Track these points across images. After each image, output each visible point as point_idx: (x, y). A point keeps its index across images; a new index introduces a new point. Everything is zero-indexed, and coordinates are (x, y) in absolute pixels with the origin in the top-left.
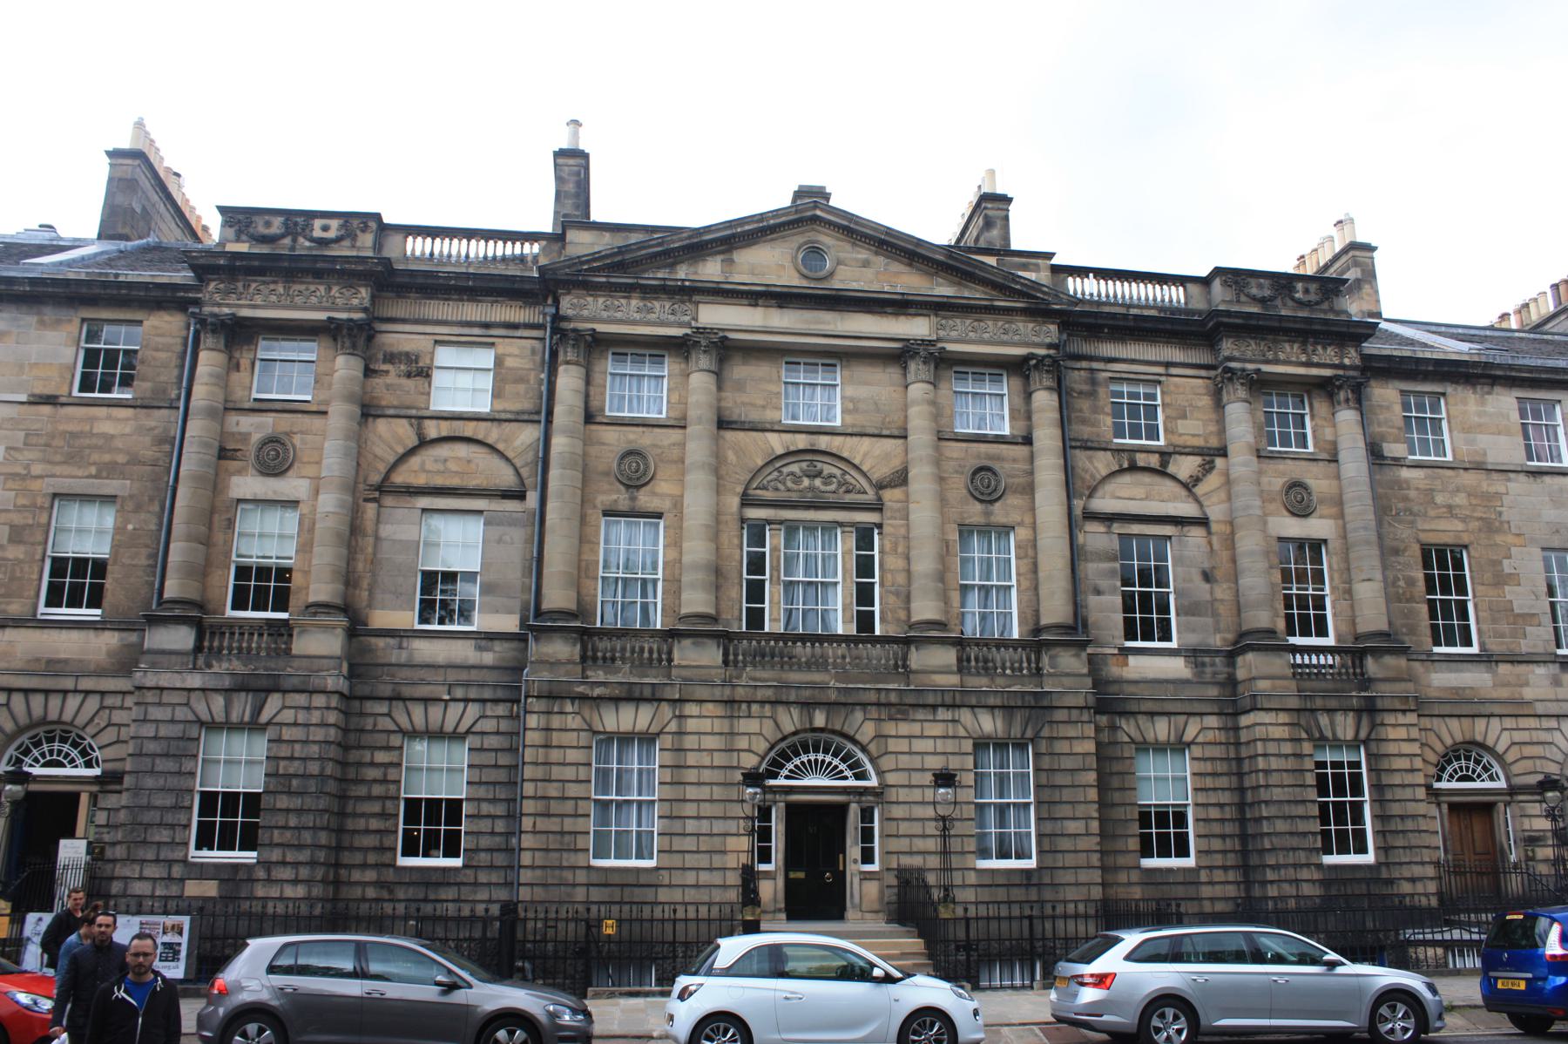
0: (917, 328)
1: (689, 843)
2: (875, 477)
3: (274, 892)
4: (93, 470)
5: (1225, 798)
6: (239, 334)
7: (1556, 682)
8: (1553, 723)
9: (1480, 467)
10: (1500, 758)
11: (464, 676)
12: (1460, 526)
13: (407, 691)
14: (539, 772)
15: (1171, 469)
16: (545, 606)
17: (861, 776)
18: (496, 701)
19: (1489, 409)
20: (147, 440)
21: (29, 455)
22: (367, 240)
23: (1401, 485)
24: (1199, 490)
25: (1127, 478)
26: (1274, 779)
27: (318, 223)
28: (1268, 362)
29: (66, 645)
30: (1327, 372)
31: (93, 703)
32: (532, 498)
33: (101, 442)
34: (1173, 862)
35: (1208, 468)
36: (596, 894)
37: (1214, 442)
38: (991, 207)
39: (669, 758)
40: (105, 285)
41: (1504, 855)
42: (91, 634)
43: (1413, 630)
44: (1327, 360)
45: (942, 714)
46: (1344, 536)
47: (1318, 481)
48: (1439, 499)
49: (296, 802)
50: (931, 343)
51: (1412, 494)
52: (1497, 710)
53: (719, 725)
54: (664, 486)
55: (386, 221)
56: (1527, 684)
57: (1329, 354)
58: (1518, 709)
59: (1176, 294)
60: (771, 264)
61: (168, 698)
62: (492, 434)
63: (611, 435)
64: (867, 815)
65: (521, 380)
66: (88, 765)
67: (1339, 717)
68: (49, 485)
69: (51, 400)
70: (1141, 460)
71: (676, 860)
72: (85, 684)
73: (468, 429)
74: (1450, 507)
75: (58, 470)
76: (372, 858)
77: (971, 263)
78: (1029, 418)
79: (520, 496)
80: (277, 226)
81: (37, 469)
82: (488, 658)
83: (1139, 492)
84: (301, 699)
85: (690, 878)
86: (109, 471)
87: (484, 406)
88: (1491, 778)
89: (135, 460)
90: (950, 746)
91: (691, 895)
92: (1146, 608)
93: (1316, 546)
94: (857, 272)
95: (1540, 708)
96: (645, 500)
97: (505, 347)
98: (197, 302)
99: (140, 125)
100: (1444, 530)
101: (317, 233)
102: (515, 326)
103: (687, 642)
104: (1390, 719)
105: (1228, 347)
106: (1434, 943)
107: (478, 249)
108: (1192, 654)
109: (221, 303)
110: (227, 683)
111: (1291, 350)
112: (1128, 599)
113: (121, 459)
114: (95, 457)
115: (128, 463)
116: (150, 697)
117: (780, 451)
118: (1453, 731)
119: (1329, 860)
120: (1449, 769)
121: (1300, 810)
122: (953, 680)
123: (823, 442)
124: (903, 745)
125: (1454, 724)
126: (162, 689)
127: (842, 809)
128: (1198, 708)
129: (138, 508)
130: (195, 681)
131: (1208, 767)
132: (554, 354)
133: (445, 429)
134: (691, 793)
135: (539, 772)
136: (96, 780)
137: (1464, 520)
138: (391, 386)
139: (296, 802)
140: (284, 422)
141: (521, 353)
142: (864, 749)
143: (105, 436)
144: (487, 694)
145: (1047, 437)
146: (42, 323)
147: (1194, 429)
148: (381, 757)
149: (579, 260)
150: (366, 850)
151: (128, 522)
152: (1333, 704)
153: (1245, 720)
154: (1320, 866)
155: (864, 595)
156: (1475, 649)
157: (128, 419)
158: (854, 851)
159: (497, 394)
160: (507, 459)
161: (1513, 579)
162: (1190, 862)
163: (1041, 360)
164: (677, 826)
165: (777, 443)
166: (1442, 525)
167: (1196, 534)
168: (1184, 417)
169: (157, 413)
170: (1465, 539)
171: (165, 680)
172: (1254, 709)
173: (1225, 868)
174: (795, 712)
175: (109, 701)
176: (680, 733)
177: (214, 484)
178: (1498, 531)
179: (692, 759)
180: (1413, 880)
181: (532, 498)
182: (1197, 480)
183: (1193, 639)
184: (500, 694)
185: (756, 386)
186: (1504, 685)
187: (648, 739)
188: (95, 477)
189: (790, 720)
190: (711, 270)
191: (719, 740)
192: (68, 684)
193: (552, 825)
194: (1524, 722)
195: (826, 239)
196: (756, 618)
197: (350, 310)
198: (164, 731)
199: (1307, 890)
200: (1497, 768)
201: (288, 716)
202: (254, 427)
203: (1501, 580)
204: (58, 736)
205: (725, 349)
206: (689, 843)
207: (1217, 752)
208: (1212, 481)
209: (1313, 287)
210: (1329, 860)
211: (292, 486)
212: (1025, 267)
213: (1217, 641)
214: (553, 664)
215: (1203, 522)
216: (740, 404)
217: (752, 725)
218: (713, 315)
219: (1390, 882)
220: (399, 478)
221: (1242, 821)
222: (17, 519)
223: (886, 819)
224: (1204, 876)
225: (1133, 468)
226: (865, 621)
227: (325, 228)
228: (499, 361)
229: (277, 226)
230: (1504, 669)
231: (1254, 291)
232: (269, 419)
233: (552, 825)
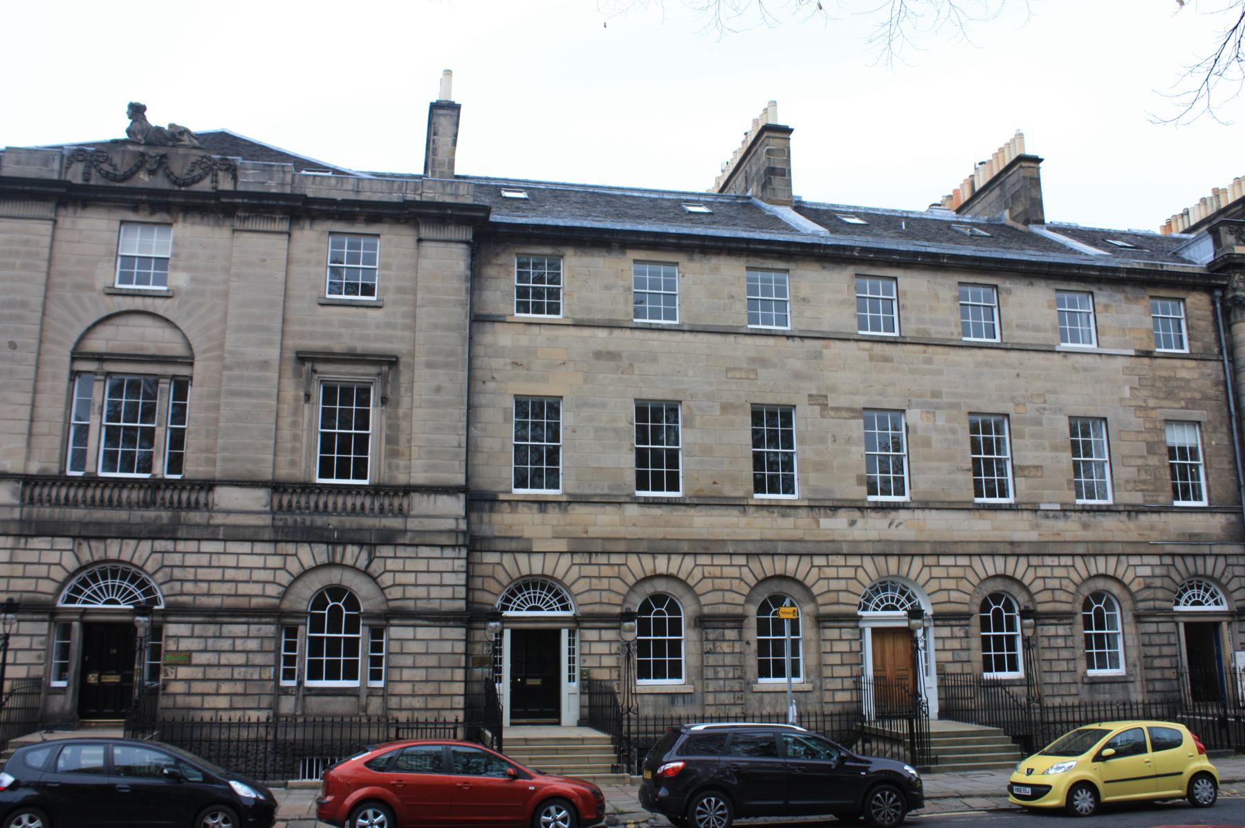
29: (1199, 524)
33: (1183, 384)
113: (1197, 396)
114: (1182, 394)
115: (1202, 399)
143: (1182, 379)
151: (1211, 439)
157: (1193, 368)
188: (1186, 408)
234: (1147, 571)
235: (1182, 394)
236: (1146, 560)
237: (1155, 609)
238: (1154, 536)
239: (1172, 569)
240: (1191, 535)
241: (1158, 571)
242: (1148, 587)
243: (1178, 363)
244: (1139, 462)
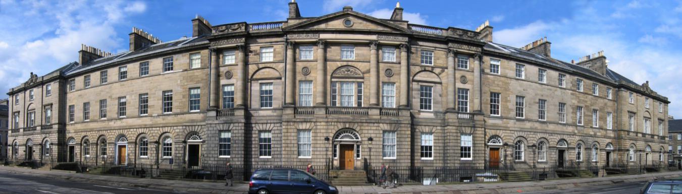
1: (318, 153)
2: (363, 71)
4: (195, 82)
5: (441, 145)
7: (515, 124)
8: (513, 132)
10: (502, 139)
11: (270, 118)
12: (500, 89)
13: (258, 122)
14: (286, 138)
15: (434, 71)
18: (277, 123)
20: (204, 75)
22: (243, 28)
23: (488, 79)
24: (440, 76)
25: (423, 73)
26: (451, 141)
28: (459, 49)
29: (194, 117)
30: (473, 52)
32: (283, 79)
34: (428, 158)
35: (443, 71)
36: (298, 164)
37: (445, 66)
39: (314, 135)
41: (500, 159)
43: (486, 111)
44: (474, 50)
45: (376, 125)
47: (469, 76)
48: (496, 82)
49: (237, 145)
50: (376, 41)
51: (490, 81)
52: (502, 128)
53: (324, 127)
54: (312, 74)
56: (509, 123)
57: (474, 48)
58: (506, 129)
64: (358, 147)
65: (279, 53)
66: (200, 139)
69: (186, 70)
70: (427, 69)
71: (315, 157)
73: (268, 65)
74: (498, 85)
75: (189, 83)
77: (388, 23)
78: (400, 58)
79: (280, 78)
81: (186, 84)
82: (275, 114)
83: (426, 76)
84: (237, 124)
85: (319, 160)
86: (198, 82)
87: (271, 60)
88: (500, 143)
89: (202, 80)
90: (377, 132)
91: (318, 164)
92: (426, 102)
93: (467, 90)
94: (358, 25)
95: (511, 129)
96: (308, 78)
97: (275, 46)
98: (210, 46)
100: (496, 89)
102: (278, 42)
103: (317, 109)
105: (450, 45)
106: (482, 176)
107: (268, 27)
108: (436, 113)
111: (465, 47)
112: (422, 100)
113: (200, 79)
114: (195, 80)
117: (340, 66)
118: (493, 132)
120: (491, 141)
121: (456, 148)
122: (379, 117)
123: (350, 64)
124: (366, 132)
127: (353, 145)
128: (435, 125)
129: (204, 89)
131: (437, 138)
132: (286, 47)
133: (263, 65)
134: (319, 142)
135: (286, 138)
136: (202, 142)
137: (501, 88)
139: (237, 145)
141: (280, 48)
142: (358, 132)
144: (275, 122)
145: (404, 62)
146: (183, 56)
147: (441, 62)
149: (291, 26)
153: (446, 128)
154: (460, 160)
155: (359, 98)
156: (499, 115)
159: (274, 57)
162: (432, 158)
163: (403, 45)
164: (315, 149)
165: (339, 64)
166: (496, 88)
167: (439, 86)
168: (438, 59)
169: (206, 69)
170: (500, 92)
172: (448, 126)
173: (440, 160)
174: (342, 124)
178: (508, 91)
179: (319, 135)
180: (479, 164)
181: (283, 79)
182: (440, 74)
183: (436, 109)
184: (278, 121)
185: (333, 52)
186: (505, 123)
187: (309, 130)
189: (341, 126)
191: (326, 128)
193: (289, 149)
195: (351, 18)
196: (334, 103)
199: (456, 165)
200: (501, 141)
201: (234, 128)
204: (193, 134)
206: (318, 153)
207: (440, 135)
208: (444, 74)
212: (401, 24)
213: (441, 110)
214: (288, 115)
215: (440, 83)
217: (332, 127)
218: (323, 36)
219: (474, 164)
221: (444, 150)
222: (184, 94)
223: (362, 148)
224: (435, 162)
225: (425, 70)
226: (359, 104)
228: (274, 50)
230: (505, 120)
233: (289, 149)
238: (181, 120)
240: (192, 120)
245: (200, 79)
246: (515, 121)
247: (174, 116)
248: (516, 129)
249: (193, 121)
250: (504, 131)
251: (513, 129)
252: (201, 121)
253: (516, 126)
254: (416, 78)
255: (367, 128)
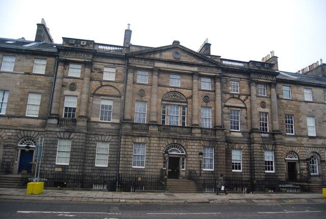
0: (195, 69)
1: (151, 164)
2: (186, 97)
3: (72, 171)
5: (248, 159)
6: (66, 63)
7: (308, 141)
9: (296, 100)
11: (109, 131)
12: (292, 111)
13: (98, 133)
14: (123, 149)
15: (240, 98)
16: (125, 118)
17: (182, 152)
18: (115, 136)
19: (298, 89)
21: (25, 84)
22: (92, 46)
23: (281, 103)
24: (245, 102)
25: (232, 99)
26: (257, 156)
27: (82, 42)
28: (259, 79)
30: (270, 81)
31: (37, 133)
32: (122, 98)
35: (247, 98)
36: (133, 173)
37: (248, 93)
38: (207, 46)
39: (147, 148)
40: (40, 52)
41: (297, 172)
42: (36, 120)
43: (283, 130)
44: (269, 79)
45: (198, 141)
46: (271, 112)
47: (267, 102)
48: (289, 106)
49: (77, 154)
50: (198, 72)
51: (284, 105)
53: (157, 142)
55: (95, 42)
57: (270, 78)
58: (301, 146)
59: (241, 65)
60: (168, 55)
61: (52, 133)
62: (115, 85)
63: (138, 86)
64: (183, 160)
65: (121, 75)
67: (269, 145)
68: (28, 90)
70: (235, 96)
71: (148, 167)
72: (35, 129)
73: (111, 84)
76: (91, 165)
78: (215, 87)
79: (120, 97)
80: (74, 42)
81: (26, 87)
82: (114, 127)
84: (78, 134)
85: (151, 170)
86: (40, 88)
87: (113, 79)
90: (199, 147)
91: (151, 173)
93: (266, 113)
94: (184, 58)
95: (305, 145)
97: (118, 68)
98: (58, 56)
99: (43, 19)
100: (289, 111)
101: (82, 44)
102: (120, 65)
103: (151, 126)
104: (278, 146)
105: (252, 76)
106: (285, 188)
108: (243, 132)
109: (63, 56)
110: (64, 130)
111: (263, 77)
112: (231, 121)
113: (43, 86)
114: (37, 85)
116: (49, 132)
117: (169, 91)
118: (290, 149)
119: (266, 171)
121: (262, 162)
123: (177, 90)
124: (190, 147)
125: (289, 148)
126: (51, 131)
127: (179, 158)
128: (243, 142)
130: (57, 130)
131: (245, 153)
132: (127, 70)
133: (106, 83)
134: (152, 154)
135: (123, 149)
138: (96, 74)
139: (77, 154)
140: (75, 81)
141: (121, 69)
142: (183, 147)
144: (113, 134)
145: (218, 91)
146: (27, 58)
148: (92, 145)
149: (132, 53)
150: (89, 163)
152: (268, 143)
153: (252, 145)
154: (265, 173)
155: (184, 118)
156: (294, 134)
158: (181, 167)
160: (117, 89)
161: (301, 121)
162: (241, 171)
163: (218, 76)
164: (149, 160)
165: (169, 90)
166: (289, 111)
167: (244, 111)
171: (51, 129)
172: (254, 143)
173: (247, 172)
174: (171, 140)
175: (40, 133)
176: (150, 143)
177: (61, 92)
179: (152, 148)
180: (281, 176)
181: (122, 98)
182: (245, 100)
183: (243, 130)
184: (116, 134)
187: (144, 144)
189: (170, 141)
190: (157, 56)
192: (32, 129)
193: (126, 159)
194: (302, 148)
195: (179, 51)
196: (164, 122)
197: (89, 59)
198: (51, 139)
199: (262, 177)
201: (76, 137)
202: (69, 81)
203: (299, 122)
205: (160, 71)
206: (151, 164)
207: (247, 151)
208: (248, 101)
209: (268, 65)
210: (266, 171)
211: (77, 93)
212: (215, 59)
213: (246, 130)
214: (127, 129)
215: (246, 108)
216: (162, 82)
217: (163, 142)
218: (158, 65)
219: (277, 176)
220: (97, 92)
221: (251, 164)
225: (233, 97)
226: (184, 124)
227: (83, 43)
228: (117, 71)
229: (74, 42)
231: (257, 65)
232: (72, 80)
233: (126, 159)
234: (11, 134)
235: (37, 85)
236: (11, 131)
237: (10, 145)
238: (16, 124)
239: (19, 134)
240: (28, 125)
241: (14, 134)
242: (9, 138)
243: (39, 76)
244: (17, 103)
245: (43, 86)
246: (308, 138)
247: (7, 118)
248: (310, 146)
249: (29, 126)
250: (299, 148)
251: (307, 146)
252: (38, 127)
253: (309, 143)
254: (228, 104)
255: (191, 144)
